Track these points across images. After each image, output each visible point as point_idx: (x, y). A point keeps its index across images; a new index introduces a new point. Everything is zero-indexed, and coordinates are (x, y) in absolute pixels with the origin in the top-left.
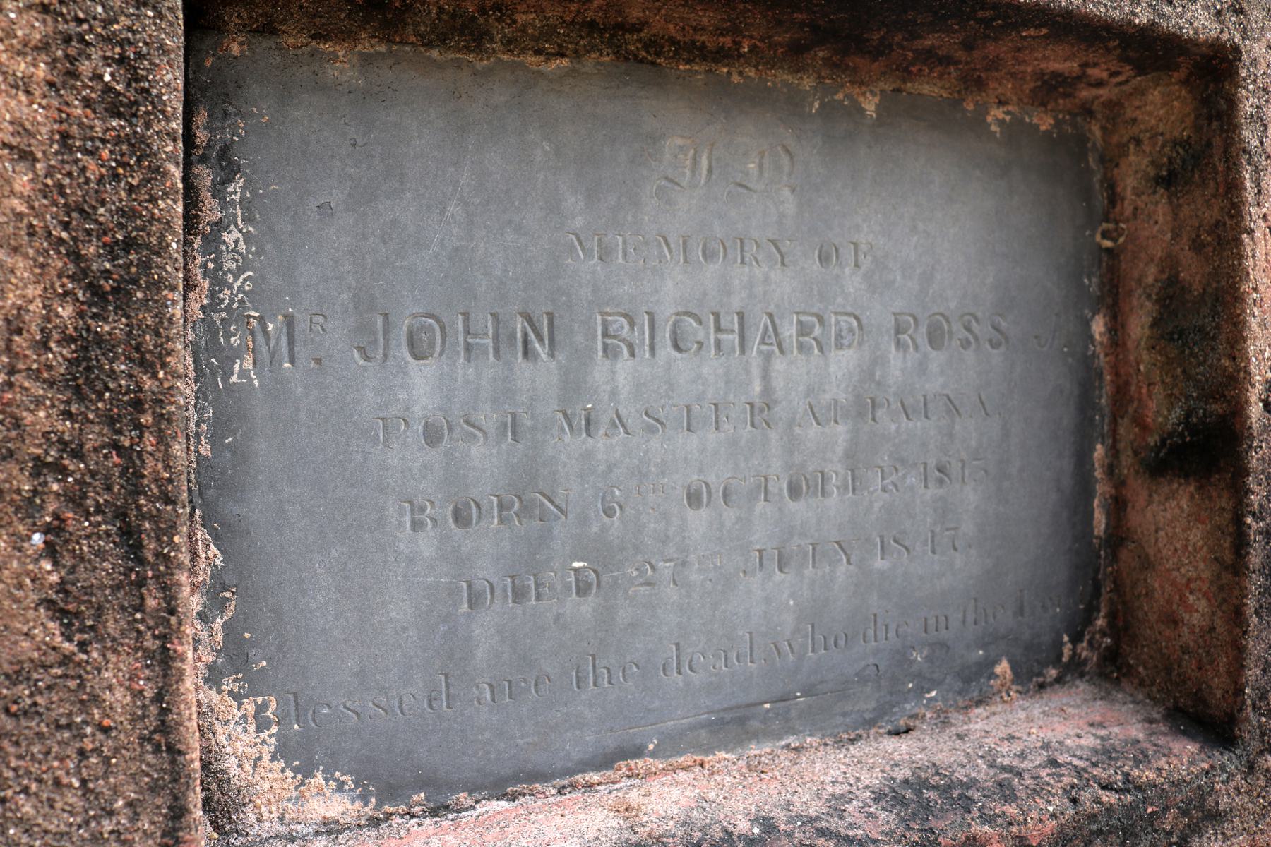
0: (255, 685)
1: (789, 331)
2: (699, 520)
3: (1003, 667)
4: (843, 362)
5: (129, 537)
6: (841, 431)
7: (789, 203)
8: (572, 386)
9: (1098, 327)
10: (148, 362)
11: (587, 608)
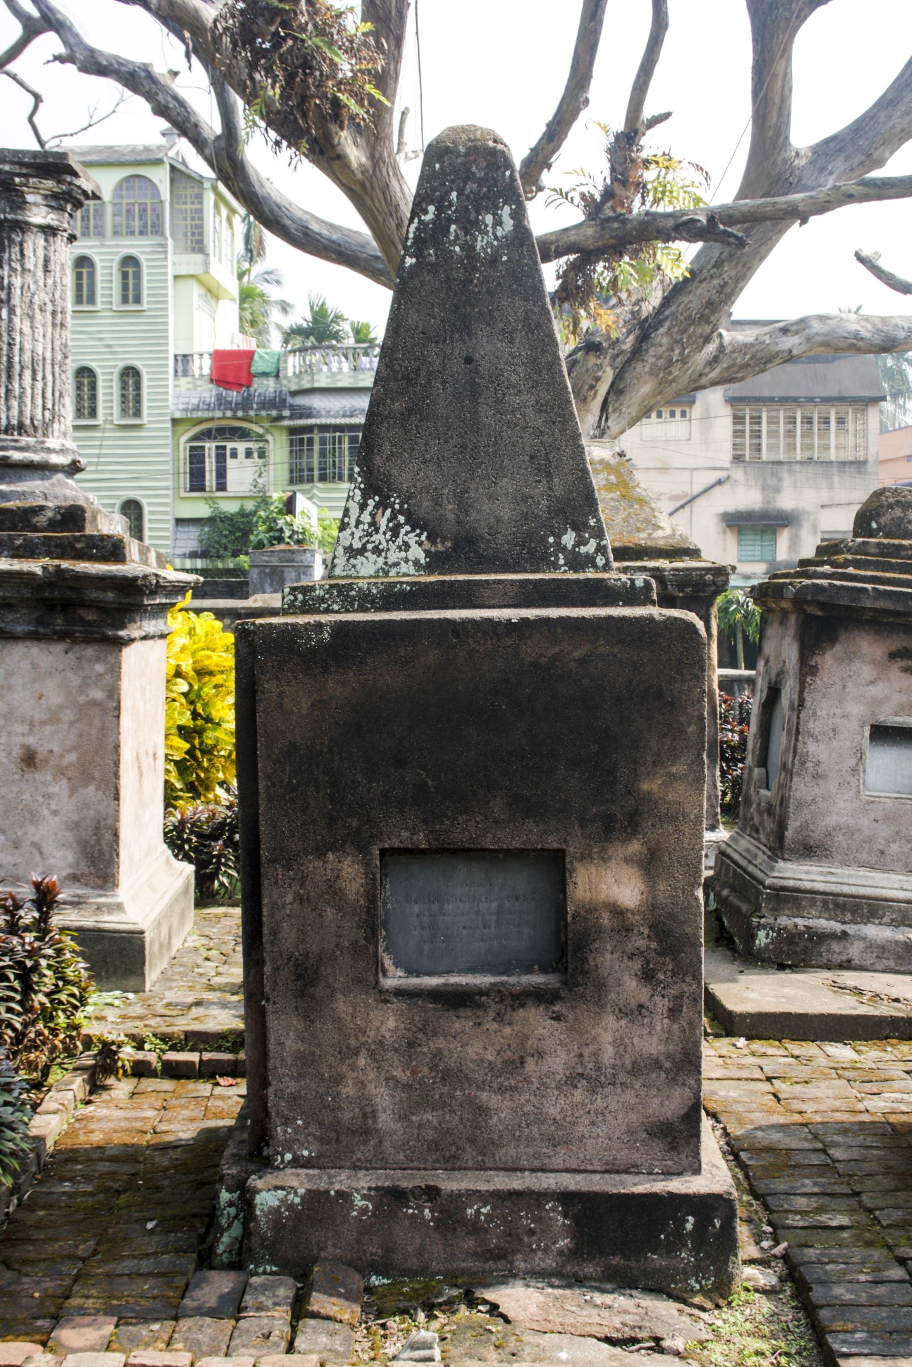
0: (390, 953)
1: (483, 898)
2: (465, 932)
3: (536, 967)
4: (494, 905)
5: (373, 931)
6: (494, 917)
7: (483, 875)
8: (441, 908)
9: (561, 896)
10: (376, 910)
11: (443, 946)
